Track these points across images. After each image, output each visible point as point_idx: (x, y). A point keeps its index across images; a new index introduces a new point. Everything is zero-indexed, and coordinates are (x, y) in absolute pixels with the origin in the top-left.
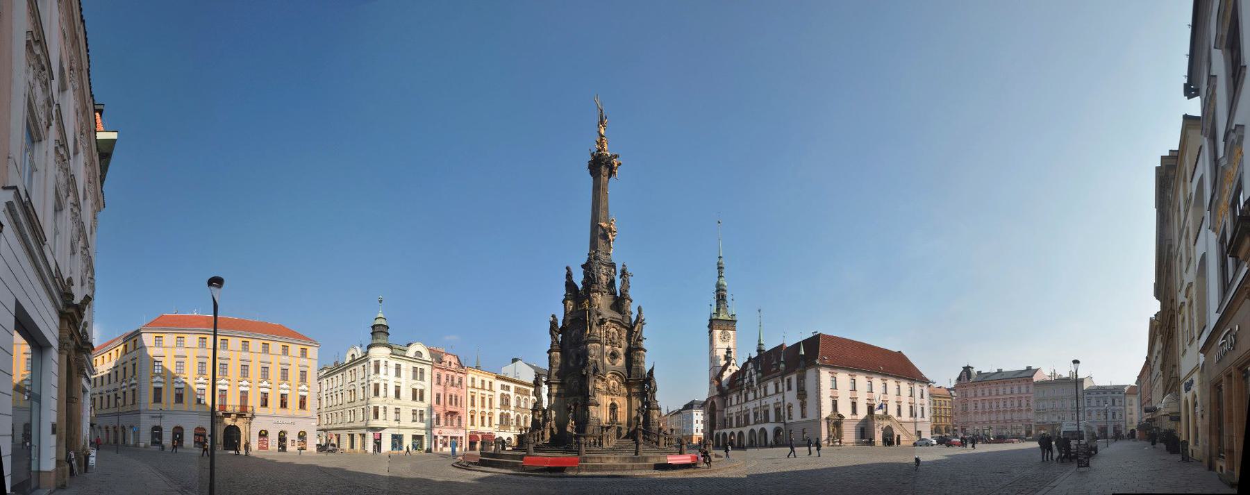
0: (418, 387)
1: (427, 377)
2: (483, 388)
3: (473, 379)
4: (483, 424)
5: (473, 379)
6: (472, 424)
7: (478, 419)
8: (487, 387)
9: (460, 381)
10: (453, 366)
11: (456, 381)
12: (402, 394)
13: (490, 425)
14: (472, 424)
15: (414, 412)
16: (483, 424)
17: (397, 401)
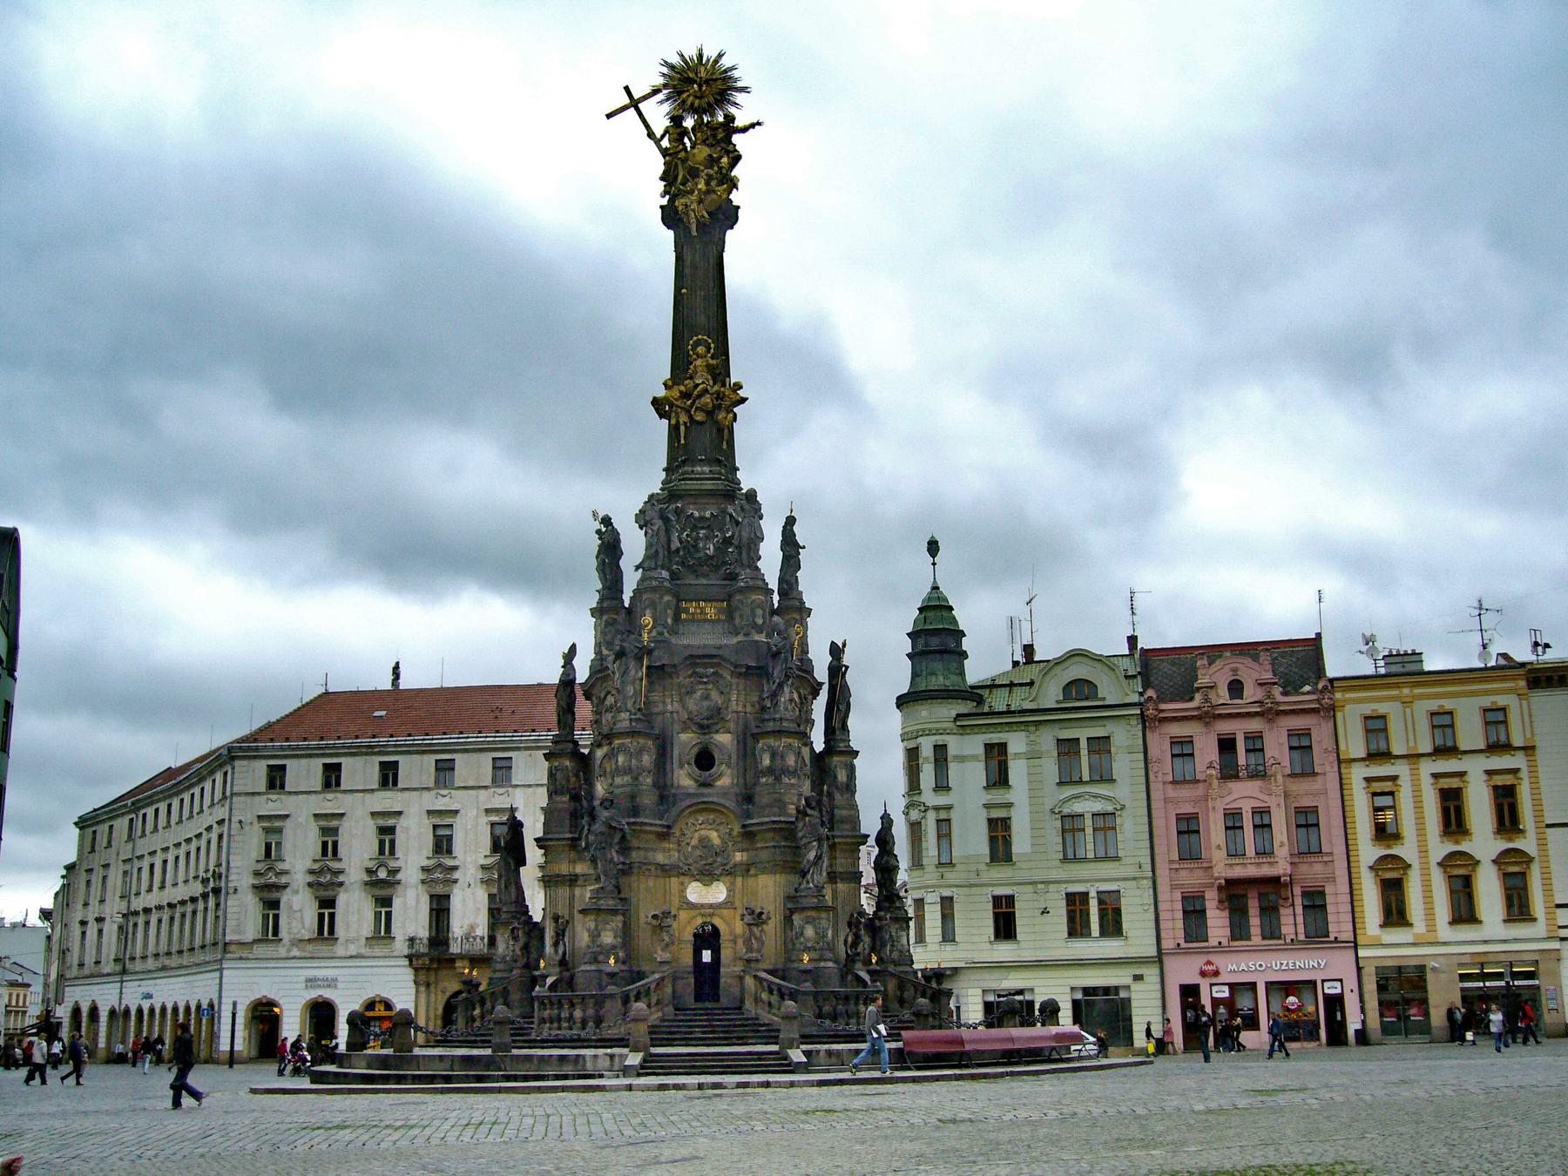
0: (1086, 807)
1: (1125, 764)
2: (1446, 750)
3: (1376, 726)
4: (1465, 912)
5: (1376, 726)
6: (1395, 914)
7: (1427, 895)
8: (1470, 734)
9: (1301, 745)
10: (1251, 693)
11: (1276, 746)
12: (1021, 843)
13: (1518, 907)
14: (1395, 914)
15: (1076, 903)
16: (1465, 912)
17: (1000, 872)
